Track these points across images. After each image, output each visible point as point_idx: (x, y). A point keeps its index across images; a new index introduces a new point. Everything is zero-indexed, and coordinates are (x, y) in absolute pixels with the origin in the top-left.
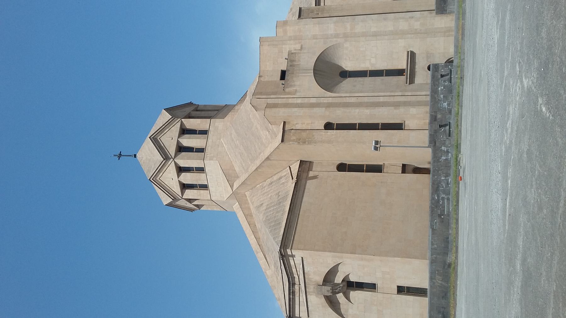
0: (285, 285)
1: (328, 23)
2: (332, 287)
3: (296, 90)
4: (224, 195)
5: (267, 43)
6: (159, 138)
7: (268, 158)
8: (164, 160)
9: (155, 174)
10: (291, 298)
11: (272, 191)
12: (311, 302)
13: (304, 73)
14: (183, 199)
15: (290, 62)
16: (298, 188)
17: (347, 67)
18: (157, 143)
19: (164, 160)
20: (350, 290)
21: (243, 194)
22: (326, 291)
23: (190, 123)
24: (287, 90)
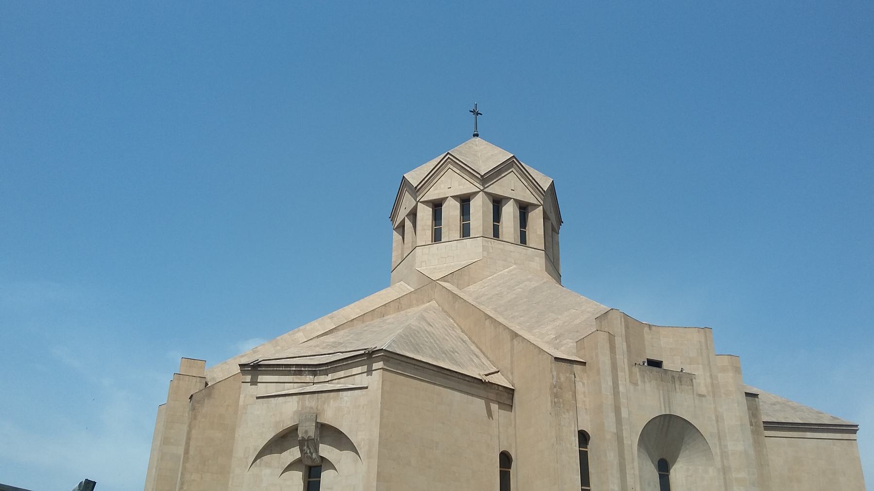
0: (310, 359)
1: (744, 441)
2: (314, 439)
3: (636, 384)
4: (425, 268)
5: (703, 340)
7: (515, 335)
8: (482, 176)
9: (457, 162)
10: (290, 368)
11: (455, 343)
13: (664, 399)
14: (417, 204)
15: (678, 376)
16: (472, 384)
17: (675, 472)
18: (507, 166)
19: (481, 175)
20: (304, 472)
21: (433, 298)
23: (536, 218)
24: (636, 370)
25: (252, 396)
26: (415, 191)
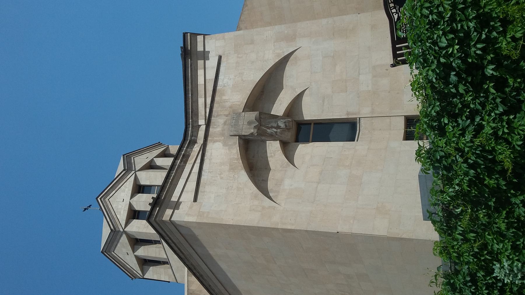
6: (133, 158)
9: (106, 191)
12: (210, 159)
22: (246, 123)
25: (191, 208)
26: (115, 235)
